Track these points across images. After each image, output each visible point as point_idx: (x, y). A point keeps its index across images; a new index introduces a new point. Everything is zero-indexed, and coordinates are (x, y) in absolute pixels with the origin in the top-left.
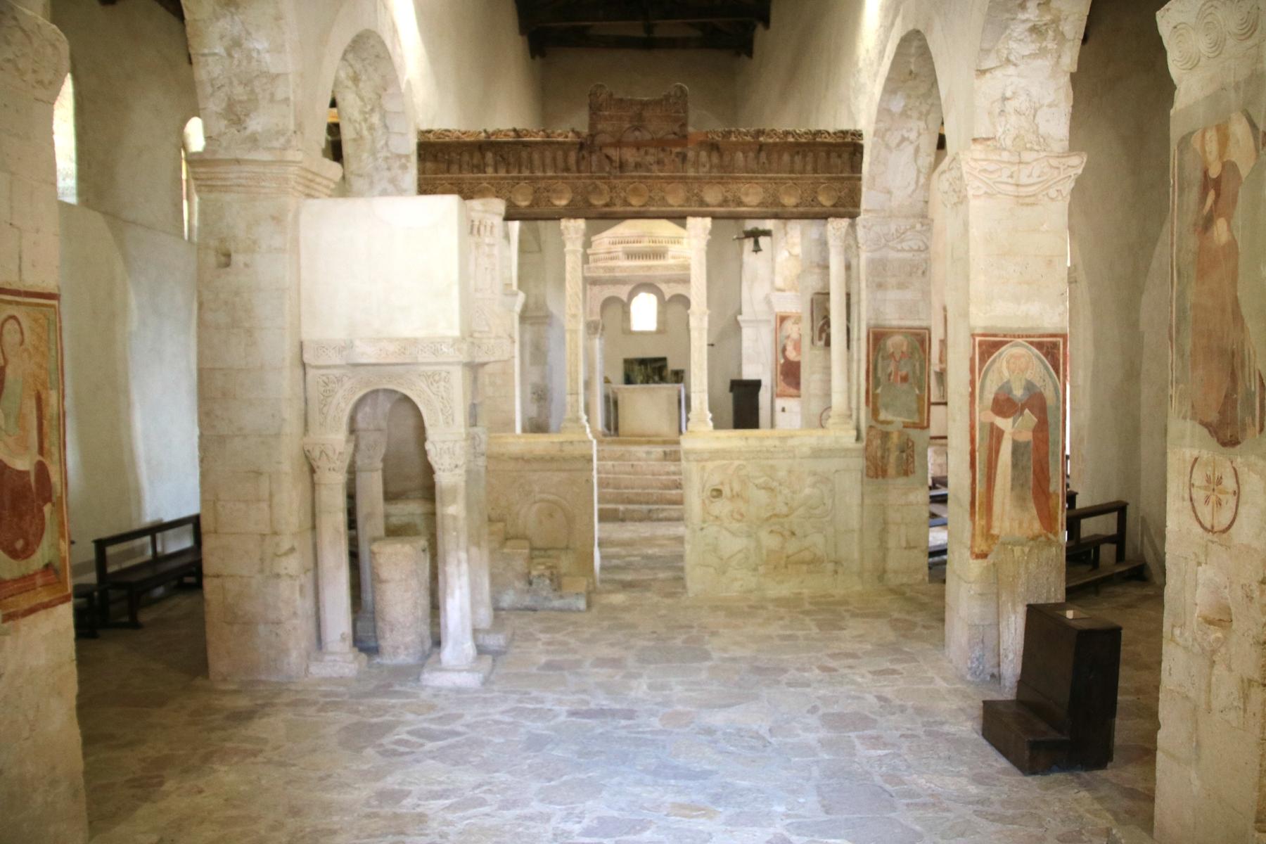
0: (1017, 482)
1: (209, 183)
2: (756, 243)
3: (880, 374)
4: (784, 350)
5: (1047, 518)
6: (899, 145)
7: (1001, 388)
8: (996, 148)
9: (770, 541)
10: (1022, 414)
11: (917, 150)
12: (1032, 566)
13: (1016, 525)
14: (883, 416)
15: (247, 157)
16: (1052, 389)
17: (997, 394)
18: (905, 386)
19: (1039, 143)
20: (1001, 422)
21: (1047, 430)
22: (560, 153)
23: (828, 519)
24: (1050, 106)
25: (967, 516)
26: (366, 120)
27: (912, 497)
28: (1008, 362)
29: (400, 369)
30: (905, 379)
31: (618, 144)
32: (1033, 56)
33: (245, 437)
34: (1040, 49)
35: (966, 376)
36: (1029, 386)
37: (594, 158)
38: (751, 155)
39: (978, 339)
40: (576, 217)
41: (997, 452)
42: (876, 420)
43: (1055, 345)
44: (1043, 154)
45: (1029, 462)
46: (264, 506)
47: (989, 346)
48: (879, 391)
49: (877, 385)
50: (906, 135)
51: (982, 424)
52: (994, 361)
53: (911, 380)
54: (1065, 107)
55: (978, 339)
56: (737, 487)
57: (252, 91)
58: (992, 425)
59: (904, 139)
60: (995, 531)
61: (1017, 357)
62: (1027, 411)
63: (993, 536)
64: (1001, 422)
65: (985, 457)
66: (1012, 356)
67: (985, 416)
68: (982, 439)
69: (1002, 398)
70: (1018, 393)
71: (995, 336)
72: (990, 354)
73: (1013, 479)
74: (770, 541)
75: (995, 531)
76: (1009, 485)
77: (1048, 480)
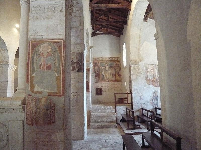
3: (35, 66)
14: (37, 89)
18: (49, 72)
30: (49, 68)
42: (33, 92)
48: (34, 75)
53: (53, 68)
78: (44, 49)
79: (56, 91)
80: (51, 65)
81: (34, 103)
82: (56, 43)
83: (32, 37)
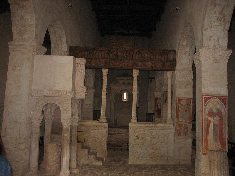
1: (13, 50)
2: (151, 80)
3: (179, 109)
4: (157, 106)
5: (223, 145)
6: (185, 53)
8: (208, 49)
9: (151, 151)
11: (189, 54)
12: (219, 157)
14: (180, 120)
15: (22, 44)
19: (220, 47)
20: (210, 118)
22: (103, 53)
23: (166, 145)
24: (222, 38)
25: (201, 143)
26: (57, 42)
27: (187, 141)
29: (56, 98)
30: (186, 111)
31: (117, 51)
32: (218, 26)
33: (15, 112)
34: (220, 24)
35: (201, 106)
36: (218, 109)
37: (111, 54)
38: (149, 55)
40: (106, 68)
43: (224, 99)
44: (221, 50)
46: (18, 130)
47: (207, 98)
48: (179, 114)
49: (179, 111)
50: (187, 51)
51: (205, 119)
54: (226, 39)
55: (204, 96)
56: (142, 136)
57: (25, 28)
58: (208, 119)
59: (186, 52)
60: (209, 148)
64: (210, 118)
67: (206, 117)
68: (205, 123)
70: (215, 111)
71: (208, 96)
73: (213, 134)
74: (151, 151)
75: (209, 148)
77: (223, 134)
78: (183, 102)
79: (188, 121)
80: (186, 110)
81: (179, 126)
82: (188, 100)
83: (178, 96)
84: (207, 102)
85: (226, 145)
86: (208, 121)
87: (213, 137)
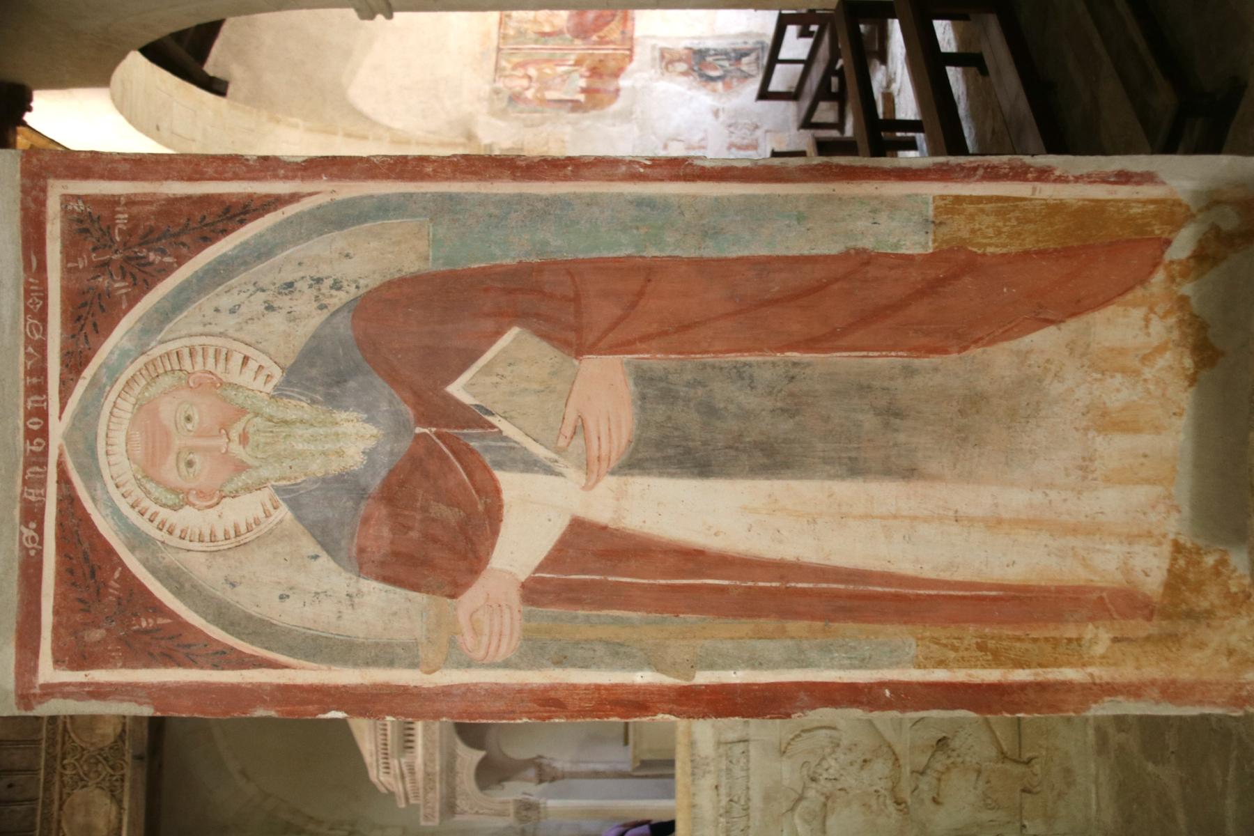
0: (868, 447)
7: (326, 540)
10: (476, 418)
13: (1113, 449)
16: (338, 240)
17: (364, 564)
20: (527, 531)
21: (572, 269)
28: (182, 498)
36: (318, 375)
39: (48, 672)
41: (692, 558)
45: (751, 377)
51: (535, 650)
52: (176, 580)
58: (533, 592)
61: (154, 445)
62: (458, 389)
63: (1175, 582)
65: (724, 633)
66: (148, 473)
68: (618, 653)
69: (381, 536)
70: (355, 439)
72: (135, 593)
73: (855, 469)
76: (886, 494)
77: (860, 263)
84: (157, 608)
85: (1099, 192)
86: (571, 595)
87: (910, 473)
